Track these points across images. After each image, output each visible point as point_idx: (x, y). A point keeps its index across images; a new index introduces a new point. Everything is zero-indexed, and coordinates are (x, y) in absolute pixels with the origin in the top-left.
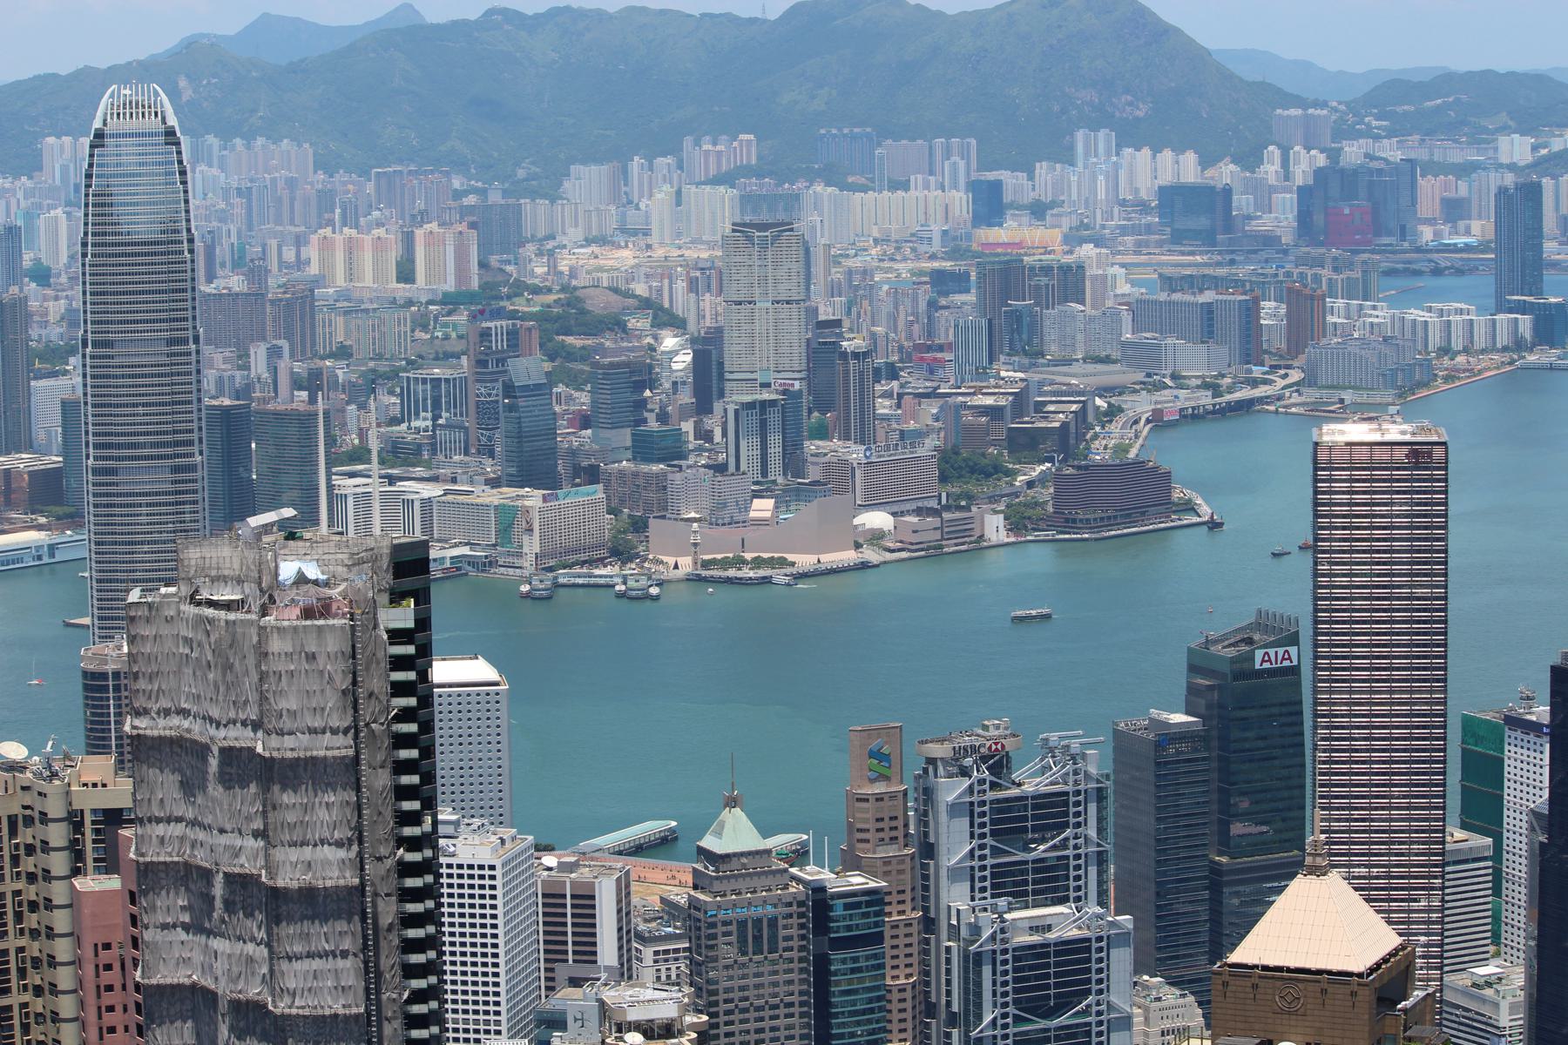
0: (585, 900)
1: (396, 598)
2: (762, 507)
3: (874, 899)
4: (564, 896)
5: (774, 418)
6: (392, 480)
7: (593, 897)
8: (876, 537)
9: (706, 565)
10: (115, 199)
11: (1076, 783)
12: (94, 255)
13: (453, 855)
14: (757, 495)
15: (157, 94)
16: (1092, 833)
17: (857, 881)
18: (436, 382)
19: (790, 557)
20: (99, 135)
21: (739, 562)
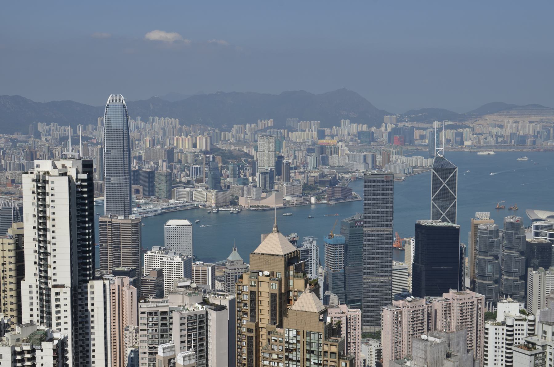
1: (84, 172)
2: (264, 195)
4: (200, 270)
5: (268, 176)
6: (185, 187)
7: (206, 271)
8: (288, 202)
9: (251, 207)
10: (111, 119)
11: (311, 248)
12: (107, 132)
13: (174, 260)
14: (263, 192)
15: (121, 97)
16: (315, 258)
18: (197, 168)
19: (269, 206)
20: (108, 105)
21: (258, 206)
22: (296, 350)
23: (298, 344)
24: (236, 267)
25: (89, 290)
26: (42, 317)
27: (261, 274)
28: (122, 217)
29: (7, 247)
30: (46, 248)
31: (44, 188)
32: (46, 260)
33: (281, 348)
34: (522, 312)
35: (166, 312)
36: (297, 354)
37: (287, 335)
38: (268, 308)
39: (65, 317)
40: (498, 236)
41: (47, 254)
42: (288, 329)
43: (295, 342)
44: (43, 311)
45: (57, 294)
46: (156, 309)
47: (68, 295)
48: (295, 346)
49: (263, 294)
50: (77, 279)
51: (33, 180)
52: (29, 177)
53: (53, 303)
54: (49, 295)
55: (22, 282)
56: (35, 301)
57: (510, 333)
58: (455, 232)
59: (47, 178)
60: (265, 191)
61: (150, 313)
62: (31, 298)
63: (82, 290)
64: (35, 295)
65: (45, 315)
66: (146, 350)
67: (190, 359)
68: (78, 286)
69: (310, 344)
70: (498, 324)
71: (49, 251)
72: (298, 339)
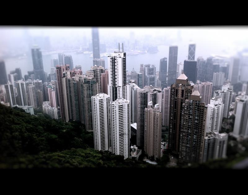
2: (132, 50)
3: (141, 75)
8: (139, 52)
17: (141, 73)
25: (125, 87)
28: (99, 59)
29: (91, 73)
30: (115, 77)
31: (114, 61)
32: (115, 80)
34: (229, 89)
38: (181, 94)
40: (205, 63)
41: (115, 78)
47: (122, 89)
49: (180, 90)
50: (123, 85)
51: (111, 58)
53: (118, 91)
54: (117, 89)
55: (108, 86)
56: (111, 90)
57: (225, 95)
58: (195, 63)
59: (115, 58)
60: (132, 49)
61: (141, 93)
62: (110, 90)
64: (111, 89)
66: (140, 102)
69: (196, 104)
70: (222, 92)
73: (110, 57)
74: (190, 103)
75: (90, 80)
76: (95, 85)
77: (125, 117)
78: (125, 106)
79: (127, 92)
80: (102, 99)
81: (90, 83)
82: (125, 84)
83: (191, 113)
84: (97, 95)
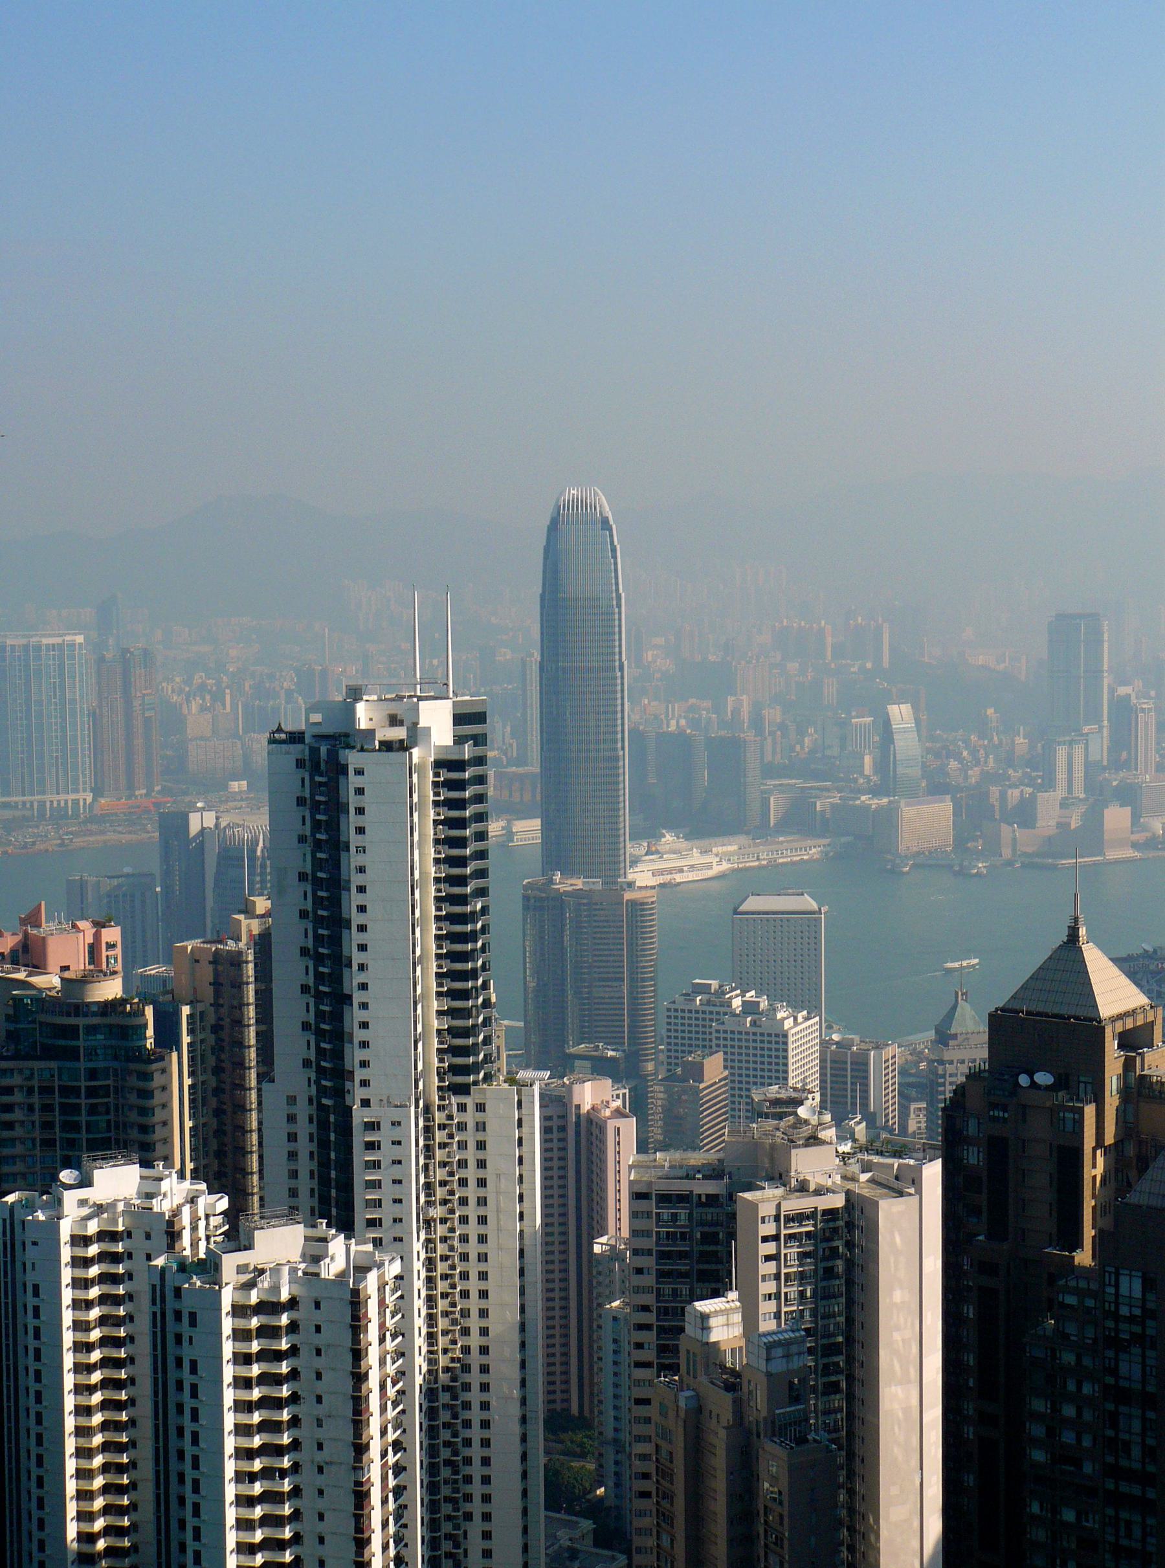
0: (861, 1066)
15: (596, 494)
22: (1140, 1339)
23: (1150, 1323)
24: (966, 1054)
25: (470, 1117)
26: (324, 1200)
27: (1024, 1080)
33: (1090, 1332)
35: (716, 1196)
36: (1144, 1356)
37: (1112, 1290)
39: (395, 1201)
42: (1113, 1270)
43: (1137, 1312)
44: (330, 1179)
45: (372, 1126)
46: (683, 1186)
48: (1138, 1329)
52: (288, 753)
56: (304, 1146)
61: (665, 1199)
63: (450, 1117)
64: (304, 1128)
65: (333, 1192)
67: (787, 1356)
68: (437, 1102)
71: (346, 991)
72: (1151, 1306)
73: (300, 747)
74: (1116, 1317)
75: (81, 1022)
76: (133, 1081)
77: (320, 1457)
78: (318, 1317)
79: (489, 1174)
80: (114, 1236)
81: (73, 1054)
82: (465, 1070)
83: (1136, 1452)
84: (66, 1176)
